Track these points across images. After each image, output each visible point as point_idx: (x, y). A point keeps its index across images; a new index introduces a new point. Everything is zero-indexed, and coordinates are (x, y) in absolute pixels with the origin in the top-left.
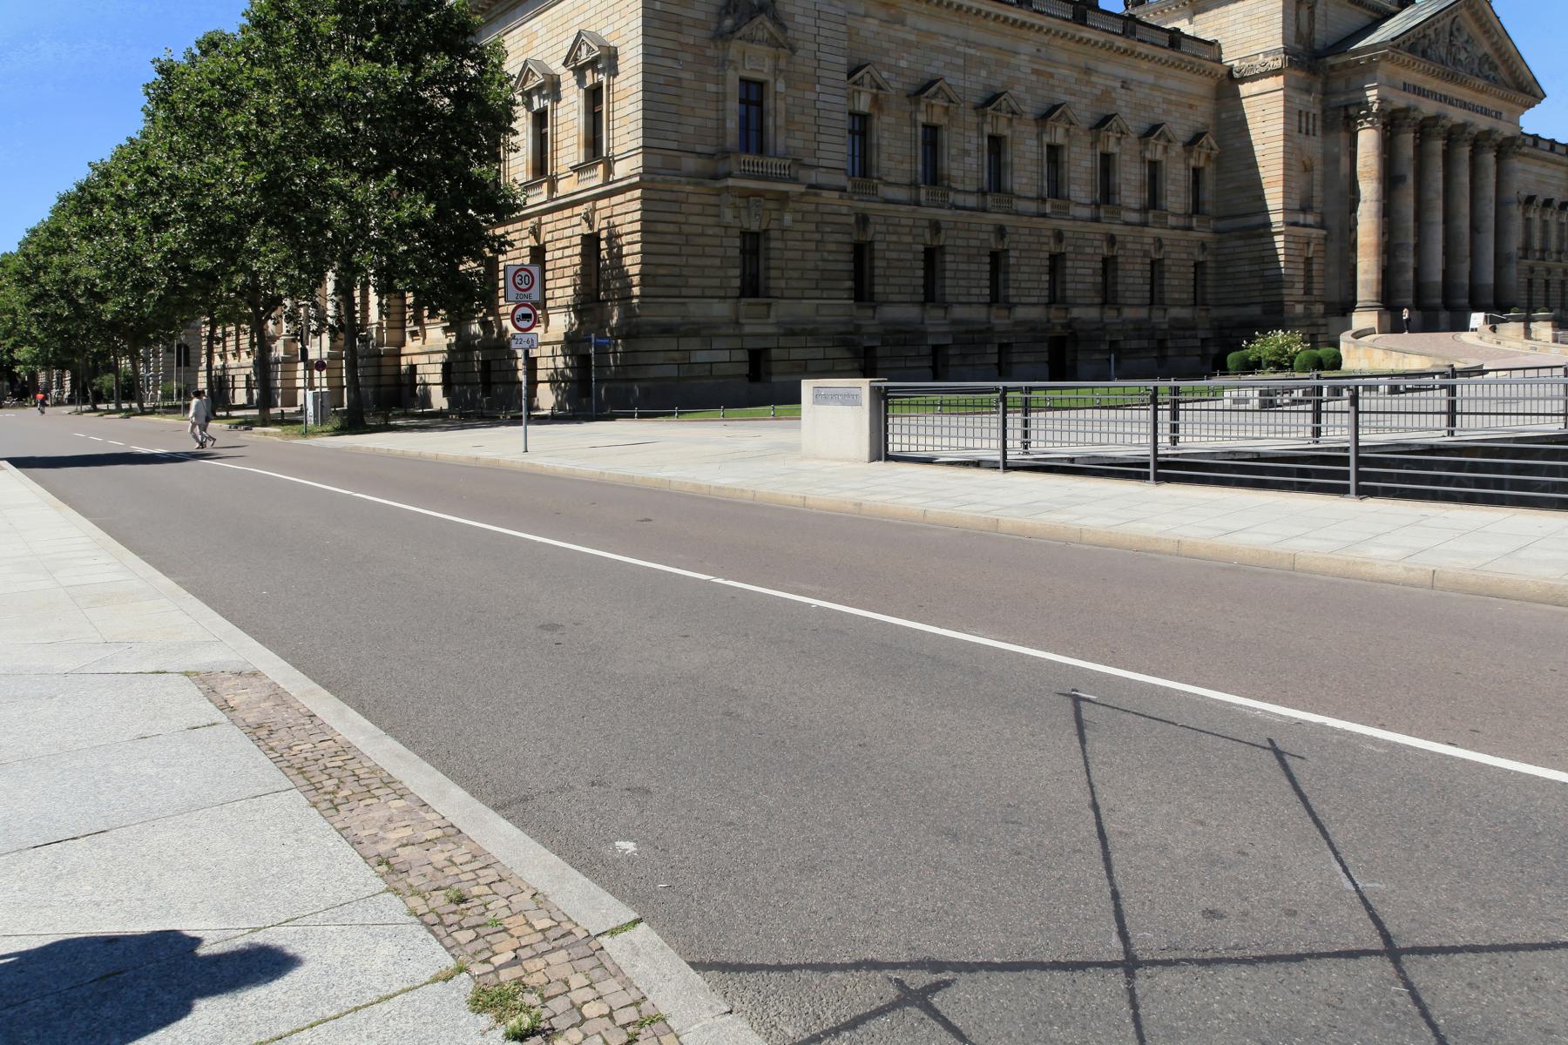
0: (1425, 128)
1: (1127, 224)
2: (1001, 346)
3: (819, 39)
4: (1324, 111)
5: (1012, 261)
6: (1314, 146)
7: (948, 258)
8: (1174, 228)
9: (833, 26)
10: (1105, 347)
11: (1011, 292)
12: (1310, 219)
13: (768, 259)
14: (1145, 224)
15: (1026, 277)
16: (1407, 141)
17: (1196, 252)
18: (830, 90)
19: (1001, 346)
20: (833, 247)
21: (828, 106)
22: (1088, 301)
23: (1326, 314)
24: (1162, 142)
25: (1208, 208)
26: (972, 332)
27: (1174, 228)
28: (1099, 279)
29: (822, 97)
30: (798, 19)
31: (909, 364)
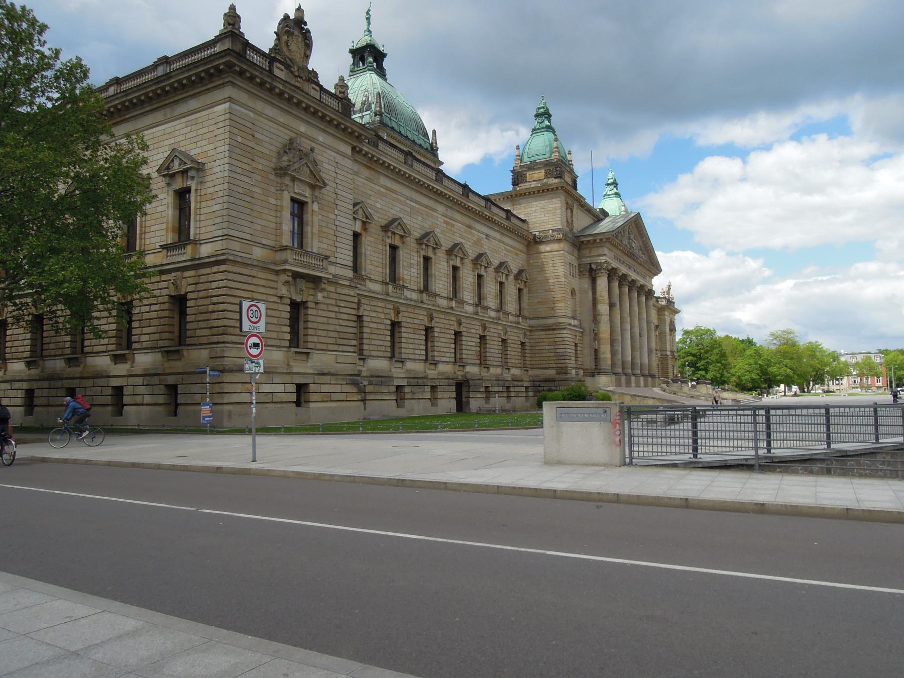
0: (623, 278)
1: (490, 318)
2: (432, 387)
3: (337, 181)
4: (579, 265)
5: (436, 334)
6: (575, 283)
7: (403, 330)
8: (511, 322)
9: (345, 174)
10: (483, 390)
11: (436, 354)
12: (576, 322)
13: (306, 321)
15: (443, 345)
16: (616, 284)
17: (521, 336)
19: (432, 387)
21: (342, 225)
22: (473, 362)
24: (506, 272)
25: (525, 313)
27: (511, 322)
28: (478, 349)
30: (325, 165)
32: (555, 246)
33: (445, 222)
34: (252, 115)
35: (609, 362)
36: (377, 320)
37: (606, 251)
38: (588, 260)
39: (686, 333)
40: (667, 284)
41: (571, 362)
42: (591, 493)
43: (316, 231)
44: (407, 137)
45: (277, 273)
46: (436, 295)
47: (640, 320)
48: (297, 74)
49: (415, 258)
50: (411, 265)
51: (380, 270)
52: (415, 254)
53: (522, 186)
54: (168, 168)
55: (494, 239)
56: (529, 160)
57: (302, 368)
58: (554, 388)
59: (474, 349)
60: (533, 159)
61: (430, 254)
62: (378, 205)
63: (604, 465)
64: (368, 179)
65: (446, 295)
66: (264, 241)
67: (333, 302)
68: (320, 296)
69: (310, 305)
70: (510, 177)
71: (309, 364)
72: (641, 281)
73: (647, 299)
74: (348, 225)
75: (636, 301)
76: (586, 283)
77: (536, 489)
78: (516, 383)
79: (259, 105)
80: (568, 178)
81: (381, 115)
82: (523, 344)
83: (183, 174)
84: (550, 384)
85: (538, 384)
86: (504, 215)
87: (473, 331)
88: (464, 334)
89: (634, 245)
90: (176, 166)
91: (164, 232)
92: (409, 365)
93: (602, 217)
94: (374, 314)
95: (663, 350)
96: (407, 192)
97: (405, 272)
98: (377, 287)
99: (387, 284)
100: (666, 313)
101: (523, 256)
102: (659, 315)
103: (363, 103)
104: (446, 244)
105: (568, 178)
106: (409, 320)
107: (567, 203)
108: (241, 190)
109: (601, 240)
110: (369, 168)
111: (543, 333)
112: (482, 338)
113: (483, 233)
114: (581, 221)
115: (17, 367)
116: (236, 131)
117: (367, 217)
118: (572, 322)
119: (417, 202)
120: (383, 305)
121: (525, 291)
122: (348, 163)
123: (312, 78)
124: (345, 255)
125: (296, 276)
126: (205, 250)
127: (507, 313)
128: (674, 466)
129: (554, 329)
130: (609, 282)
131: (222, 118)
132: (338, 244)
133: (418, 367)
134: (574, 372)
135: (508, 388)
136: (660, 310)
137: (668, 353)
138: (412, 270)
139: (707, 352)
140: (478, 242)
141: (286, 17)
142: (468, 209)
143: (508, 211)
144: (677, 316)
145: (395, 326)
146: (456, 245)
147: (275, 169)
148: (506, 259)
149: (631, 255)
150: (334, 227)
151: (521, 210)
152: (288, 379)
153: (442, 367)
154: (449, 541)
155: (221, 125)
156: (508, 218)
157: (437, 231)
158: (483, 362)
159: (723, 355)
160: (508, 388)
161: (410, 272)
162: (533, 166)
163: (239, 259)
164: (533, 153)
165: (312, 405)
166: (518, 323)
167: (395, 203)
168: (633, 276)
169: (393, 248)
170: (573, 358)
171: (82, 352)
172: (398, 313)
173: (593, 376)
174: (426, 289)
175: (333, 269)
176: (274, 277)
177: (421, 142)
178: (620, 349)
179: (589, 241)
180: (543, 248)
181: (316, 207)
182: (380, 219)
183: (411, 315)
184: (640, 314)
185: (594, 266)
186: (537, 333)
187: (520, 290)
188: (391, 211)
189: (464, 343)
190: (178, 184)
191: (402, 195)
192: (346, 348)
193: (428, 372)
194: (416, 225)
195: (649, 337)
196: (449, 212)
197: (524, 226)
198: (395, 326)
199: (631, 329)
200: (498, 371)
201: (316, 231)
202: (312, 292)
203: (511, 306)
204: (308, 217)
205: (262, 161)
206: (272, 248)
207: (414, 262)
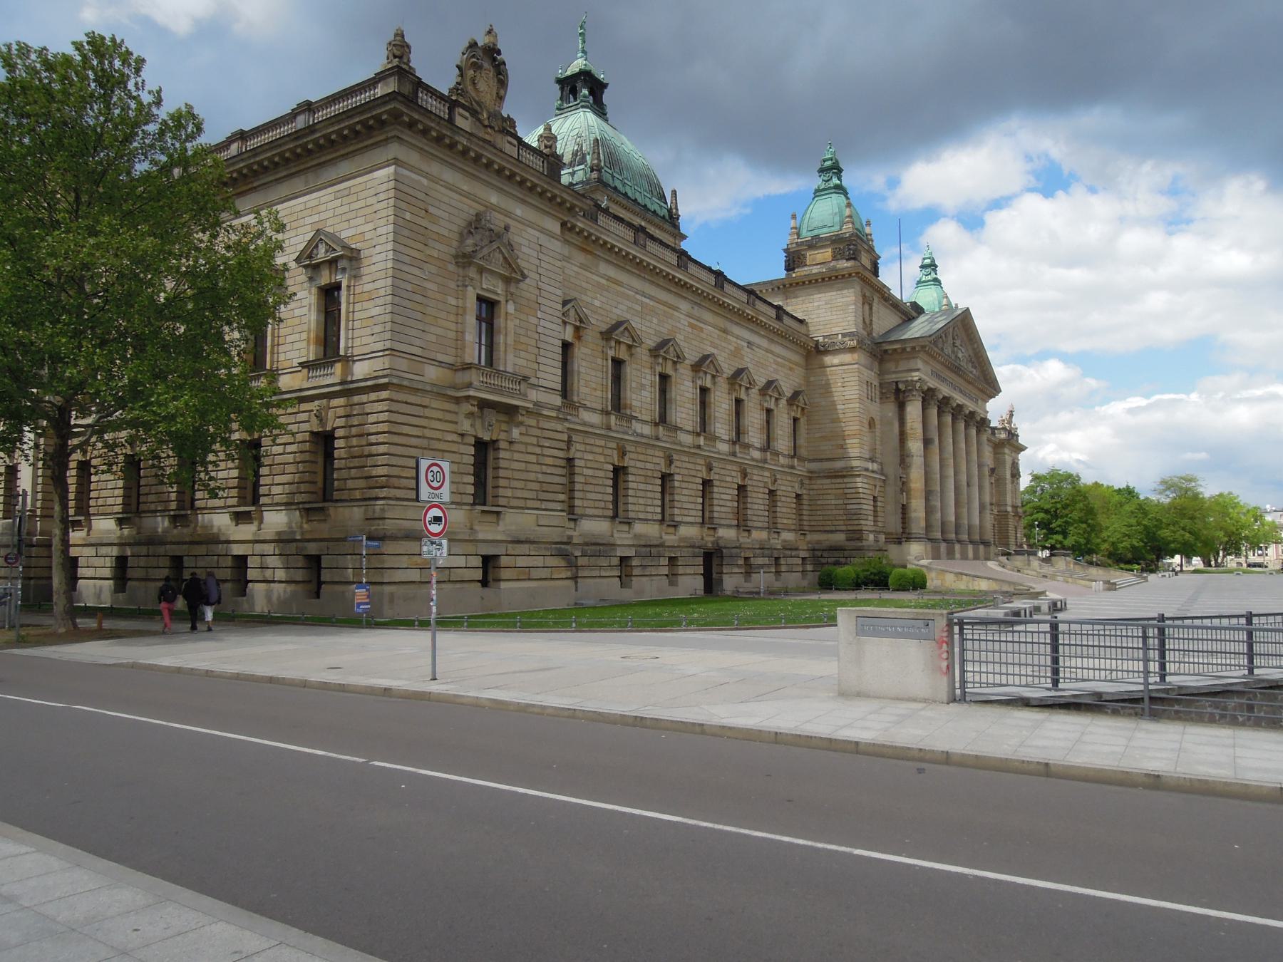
1: (753, 459)
3: (540, 271)
4: (881, 384)
5: (677, 484)
6: (875, 409)
7: (631, 478)
9: (551, 260)
10: (741, 562)
11: (676, 511)
12: (876, 467)
13: (497, 468)
14: (765, 461)
15: (686, 499)
16: (934, 412)
17: (797, 485)
18: (548, 317)
19: (671, 558)
20: (550, 461)
21: (547, 332)
22: (728, 522)
23: (887, 541)
24: (776, 395)
25: (803, 452)
26: (650, 546)
29: (542, 322)
30: (524, 249)
31: (603, 574)
32: (847, 358)
33: (691, 325)
34: (425, 181)
35: (923, 524)
36: (594, 464)
37: (920, 364)
38: (893, 377)
39: (1036, 478)
40: (1007, 409)
41: (868, 524)
42: (909, 748)
43: (510, 340)
44: (635, 201)
45: (458, 400)
46: (677, 429)
47: (968, 462)
48: (486, 123)
49: (648, 377)
50: (642, 387)
51: (599, 393)
52: (648, 371)
53: (799, 272)
54: (310, 257)
55: (759, 347)
56: (810, 234)
57: (491, 533)
58: (842, 560)
59: (729, 504)
60: (816, 232)
61: (669, 370)
62: (597, 303)
63: (925, 700)
64: (582, 266)
65: (690, 429)
66: (440, 357)
67: (534, 440)
68: (516, 433)
69: (503, 445)
70: (782, 258)
71: (500, 528)
72: (970, 406)
73: (978, 432)
74: (558, 332)
75: (963, 435)
76: (890, 410)
77: (830, 740)
78: (788, 553)
79: (435, 168)
80: (865, 260)
81: (599, 170)
82: (798, 496)
83: (332, 265)
84: (836, 554)
85: (819, 553)
86: (773, 313)
87: (728, 479)
88: (716, 483)
89: (960, 355)
90: (321, 254)
91: (304, 344)
92: (639, 528)
93: (914, 314)
94: (590, 457)
95: (1000, 504)
96: (637, 283)
97: (634, 396)
98: (595, 418)
99: (608, 413)
100: (1007, 451)
101: (800, 371)
102: (995, 453)
103: (575, 154)
104: (691, 356)
105: (865, 260)
106: (639, 465)
107: (864, 296)
108: (409, 287)
109: (913, 348)
110: (584, 250)
111: (828, 481)
112: (741, 489)
113: (743, 339)
114: (884, 320)
115: (105, 526)
116: (403, 205)
117: (581, 321)
118: (870, 466)
119: (651, 298)
120: (602, 443)
121: (803, 421)
122: (556, 246)
123: (507, 127)
124: (552, 376)
125: (484, 405)
126: (360, 370)
127: (776, 454)
128: (1026, 703)
129: (844, 476)
130: (924, 409)
131: (384, 187)
132: (541, 360)
133: (650, 530)
134: (871, 537)
135: (777, 559)
136: (998, 446)
137: (1009, 509)
138: (644, 393)
139: (1065, 507)
140: (736, 353)
141: (473, 45)
142: (722, 305)
143: (779, 308)
144: (1022, 456)
145: (619, 472)
146: (705, 358)
147: (456, 257)
148: (775, 376)
149: (957, 370)
150: (536, 336)
151: (797, 306)
152: (470, 548)
153: (684, 531)
154: (717, 826)
155: (382, 197)
156: (779, 318)
157: (679, 338)
158: (742, 524)
159: (1090, 511)
160: (777, 559)
161: (641, 396)
162: (815, 243)
163: (405, 383)
164: (815, 225)
165: (503, 585)
166: (793, 467)
167: (620, 299)
168: (959, 399)
169: (618, 363)
170: (871, 518)
171: (192, 507)
172: (623, 454)
173: (900, 543)
174: (663, 419)
175: (534, 395)
176: (453, 407)
177: (657, 208)
178: (939, 504)
179: (895, 350)
180: (829, 360)
181: (511, 308)
182: (599, 322)
183: (641, 457)
184: (968, 453)
185: (902, 386)
186: (819, 482)
187: (795, 420)
188: (614, 310)
189: (715, 496)
190: (325, 278)
191: (631, 288)
192: (551, 505)
193: (665, 537)
194: (649, 330)
195: (981, 488)
196: (697, 311)
197: (802, 329)
198: (619, 472)
199: (956, 474)
200: (763, 535)
201: (510, 340)
202: (504, 427)
203: (783, 443)
204: (500, 322)
205: (438, 246)
206: (451, 367)
207: (646, 382)
